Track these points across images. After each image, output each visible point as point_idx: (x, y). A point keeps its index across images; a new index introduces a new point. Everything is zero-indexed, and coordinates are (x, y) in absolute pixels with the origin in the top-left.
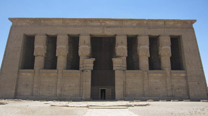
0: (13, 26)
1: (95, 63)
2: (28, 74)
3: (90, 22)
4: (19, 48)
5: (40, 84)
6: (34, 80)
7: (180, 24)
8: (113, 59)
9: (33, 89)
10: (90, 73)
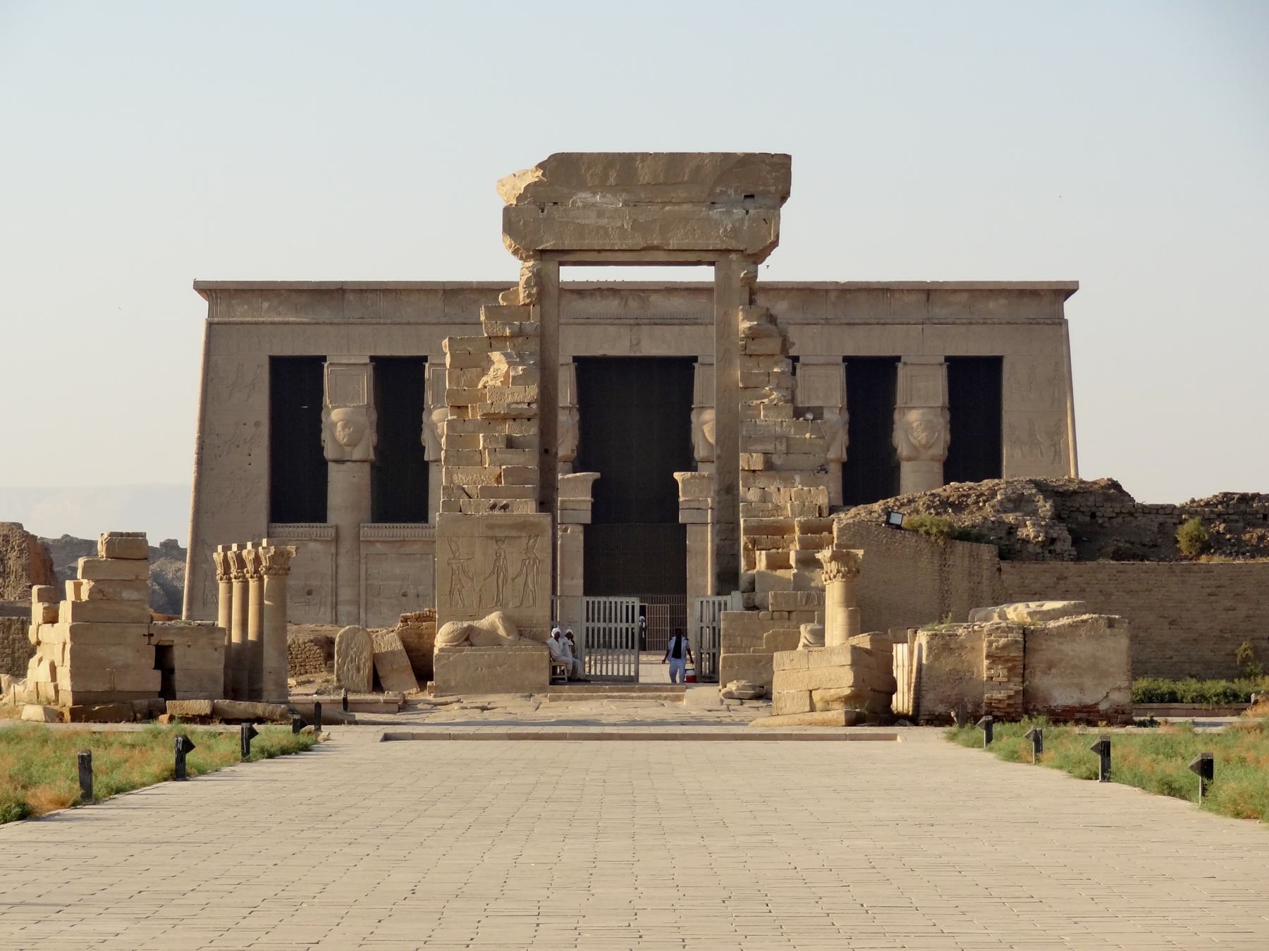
0: (216, 320)
1: (597, 488)
2: (312, 545)
3: (575, 296)
4: (257, 424)
5: (366, 585)
6: (337, 567)
7: (1002, 301)
8: (677, 476)
9: (336, 608)
10: (581, 537)
